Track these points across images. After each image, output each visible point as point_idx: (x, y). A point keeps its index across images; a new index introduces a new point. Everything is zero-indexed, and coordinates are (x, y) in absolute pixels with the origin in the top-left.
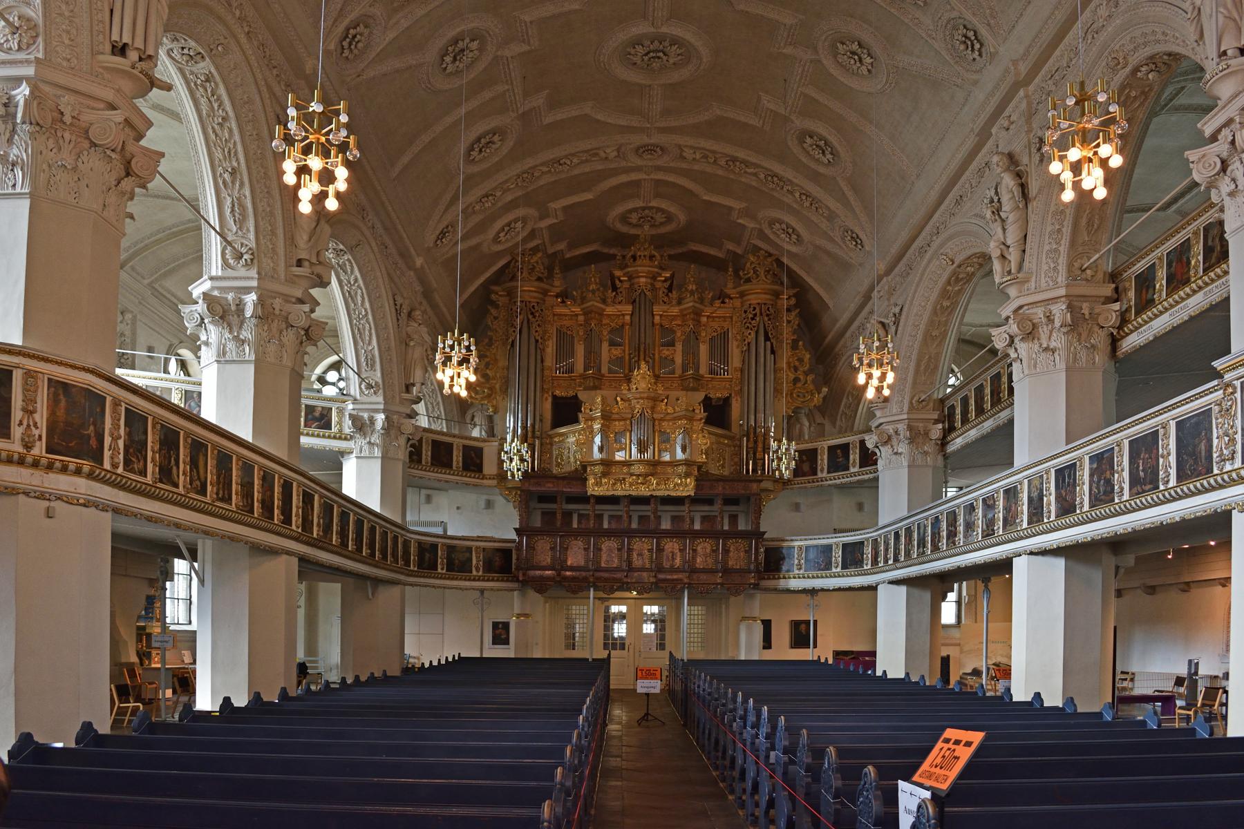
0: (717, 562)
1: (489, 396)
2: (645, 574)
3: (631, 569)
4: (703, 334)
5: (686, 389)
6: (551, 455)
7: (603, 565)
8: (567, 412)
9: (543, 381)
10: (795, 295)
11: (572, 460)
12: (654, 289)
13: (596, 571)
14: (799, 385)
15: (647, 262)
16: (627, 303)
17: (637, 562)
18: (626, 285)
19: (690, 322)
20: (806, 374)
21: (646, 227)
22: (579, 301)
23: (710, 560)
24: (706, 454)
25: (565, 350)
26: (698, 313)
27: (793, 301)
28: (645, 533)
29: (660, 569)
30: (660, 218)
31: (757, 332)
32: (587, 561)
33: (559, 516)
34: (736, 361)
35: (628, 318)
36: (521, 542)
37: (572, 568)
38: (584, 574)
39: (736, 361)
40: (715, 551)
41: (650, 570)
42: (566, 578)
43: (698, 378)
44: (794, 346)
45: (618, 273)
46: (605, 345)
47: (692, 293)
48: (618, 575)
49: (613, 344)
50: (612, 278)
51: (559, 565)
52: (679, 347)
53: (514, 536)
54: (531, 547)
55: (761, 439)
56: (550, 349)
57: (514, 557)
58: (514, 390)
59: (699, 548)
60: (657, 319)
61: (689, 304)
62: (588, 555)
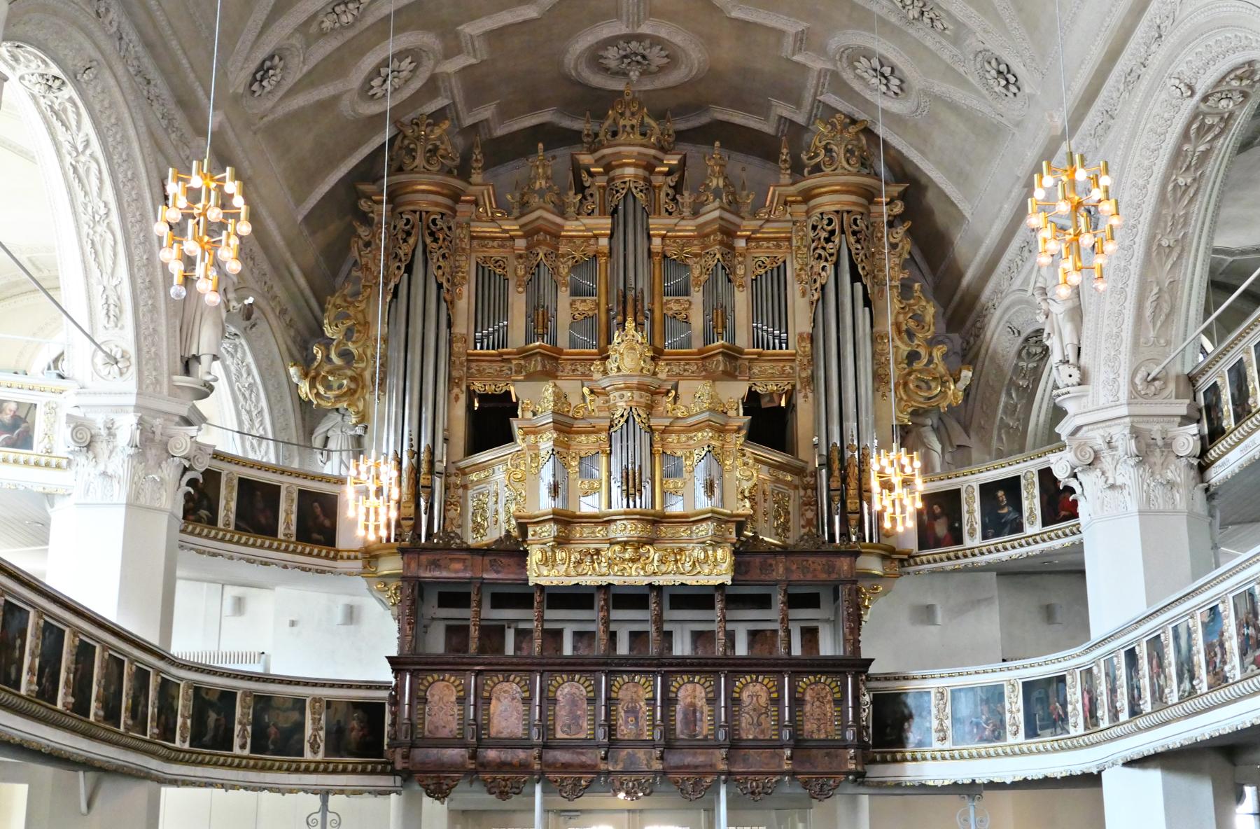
1: (351, 392)
2: (641, 754)
3: (613, 743)
4: (740, 271)
5: (712, 377)
6: (464, 507)
7: (560, 735)
8: (492, 423)
9: (451, 363)
10: (903, 196)
11: (502, 517)
12: (650, 188)
13: (546, 746)
14: (916, 366)
15: (636, 137)
16: (603, 213)
17: (625, 730)
18: (601, 181)
19: (716, 249)
20: (932, 343)
21: (634, 75)
22: (516, 212)
23: (769, 722)
24: (751, 499)
25: (490, 306)
26: (728, 233)
27: (899, 208)
28: (639, 664)
29: (669, 744)
30: (656, 57)
32: (528, 727)
33: (474, 633)
34: (800, 320)
35: (604, 242)
36: (399, 688)
37: (501, 744)
38: (521, 754)
39: (800, 319)
40: (777, 702)
41: (651, 744)
42: (484, 766)
43: (732, 354)
44: (905, 290)
45: (586, 159)
46: (564, 295)
47: (717, 194)
48: (592, 757)
49: (577, 291)
50: (577, 169)
51: (477, 736)
52: (697, 296)
53: (386, 675)
54: (419, 699)
56: (465, 304)
57: (388, 719)
58: (394, 381)
59: (745, 695)
60: (657, 242)
61: (712, 213)
62: (529, 712)
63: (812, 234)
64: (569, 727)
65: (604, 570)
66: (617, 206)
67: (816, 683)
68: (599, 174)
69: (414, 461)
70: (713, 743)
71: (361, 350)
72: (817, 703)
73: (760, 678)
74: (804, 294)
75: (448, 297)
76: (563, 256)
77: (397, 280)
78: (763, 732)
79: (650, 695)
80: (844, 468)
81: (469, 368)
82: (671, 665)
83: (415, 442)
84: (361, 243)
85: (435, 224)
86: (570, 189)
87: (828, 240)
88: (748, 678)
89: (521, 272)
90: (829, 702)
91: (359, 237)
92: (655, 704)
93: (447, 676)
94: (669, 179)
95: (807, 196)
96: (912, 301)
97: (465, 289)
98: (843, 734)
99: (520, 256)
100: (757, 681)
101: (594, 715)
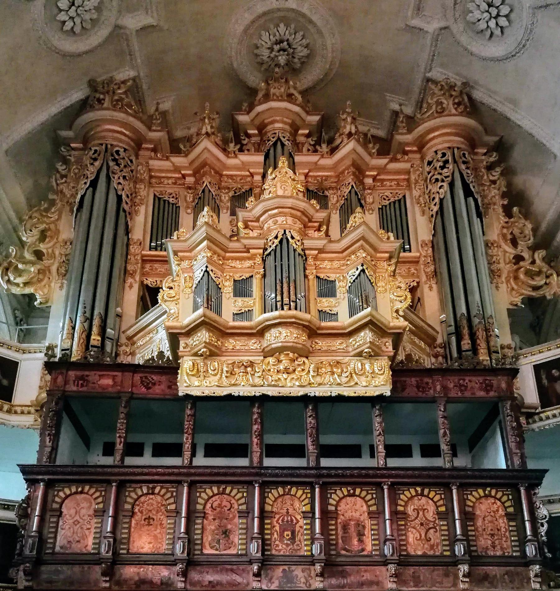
0: (453, 541)
4: (369, 199)
7: (208, 551)
16: (258, 151)
18: (256, 139)
20: (533, 249)
26: (359, 171)
27: (494, 157)
31: (452, 185)
55: (481, 334)
59: (410, 510)
61: (349, 147)
63: (427, 169)
64: (218, 542)
65: (258, 381)
66: (269, 150)
67: (486, 496)
68: (254, 135)
69: (86, 325)
70: (377, 559)
71: (50, 251)
72: (489, 518)
73: (426, 491)
74: (423, 213)
75: (126, 207)
76: (225, 188)
77: (83, 192)
78: (432, 547)
79: (308, 508)
80: (473, 336)
81: (143, 268)
82: (329, 476)
83: (88, 310)
84: (58, 175)
85: (119, 155)
86: (232, 142)
87: (442, 168)
88: (413, 491)
89: (190, 198)
90: (501, 516)
91: (58, 172)
92: (313, 517)
93: (87, 488)
94: (310, 139)
95: (421, 144)
96: (512, 220)
97: (142, 209)
98: (523, 552)
99: (190, 188)
100: (422, 495)
101: (246, 529)
